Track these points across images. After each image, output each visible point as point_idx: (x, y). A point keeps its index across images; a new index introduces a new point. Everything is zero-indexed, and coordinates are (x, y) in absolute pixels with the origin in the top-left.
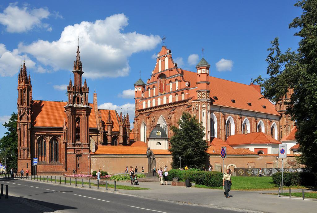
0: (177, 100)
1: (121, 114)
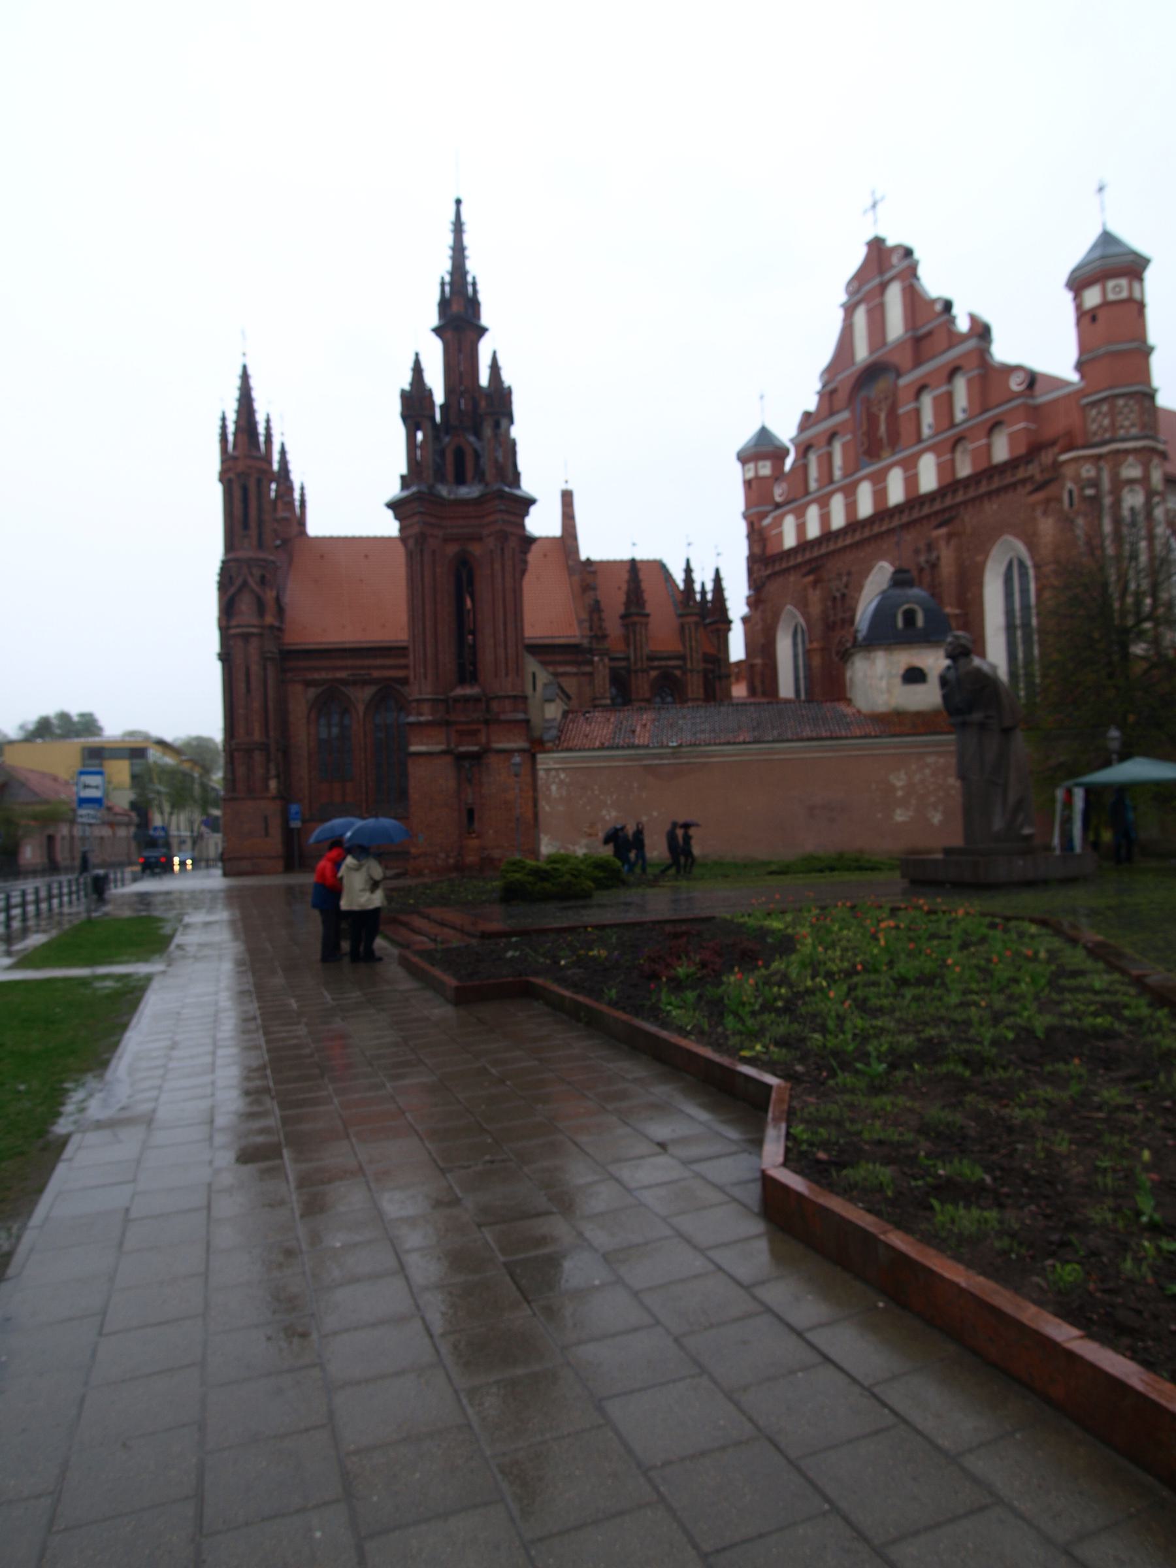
0: (964, 470)
1: (688, 571)
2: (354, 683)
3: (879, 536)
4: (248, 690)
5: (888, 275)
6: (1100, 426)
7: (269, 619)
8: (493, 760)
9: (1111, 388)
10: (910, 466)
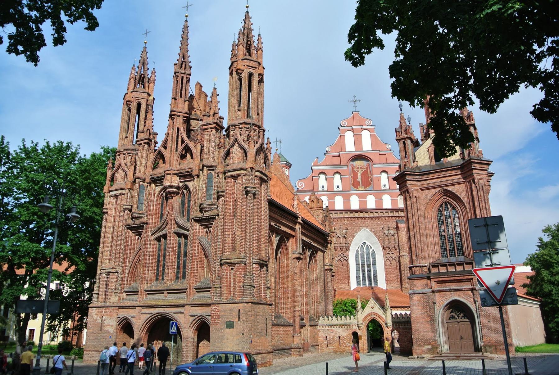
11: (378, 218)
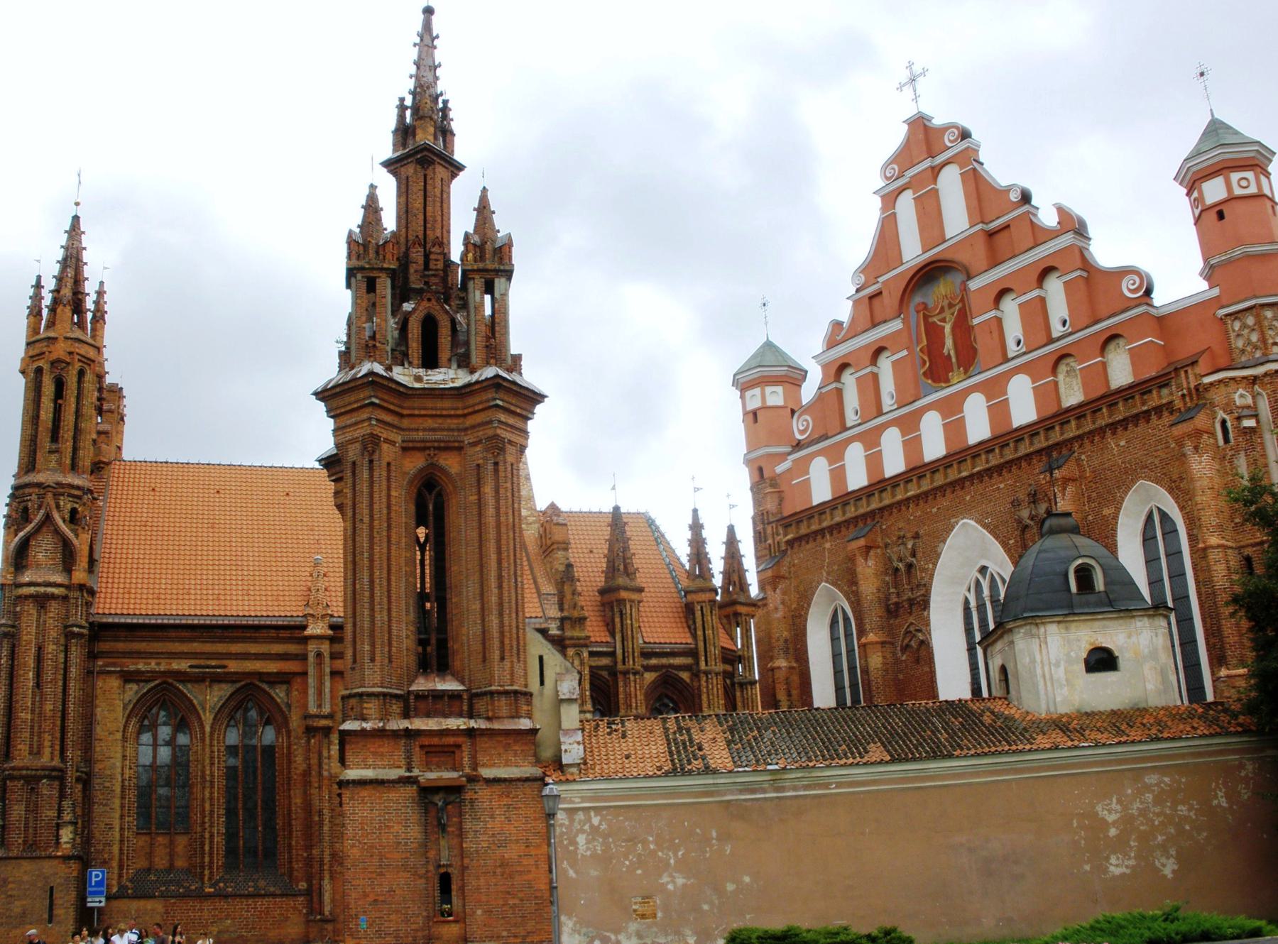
0: (1072, 395)
1: (696, 527)
2: (198, 679)
3: (960, 483)
4: (38, 685)
5: (940, 159)
6: (1249, 342)
7: (79, 576)
8: (483, 795)
9: (1256, 297)
10: (995, 389)
11: (999, 469)
